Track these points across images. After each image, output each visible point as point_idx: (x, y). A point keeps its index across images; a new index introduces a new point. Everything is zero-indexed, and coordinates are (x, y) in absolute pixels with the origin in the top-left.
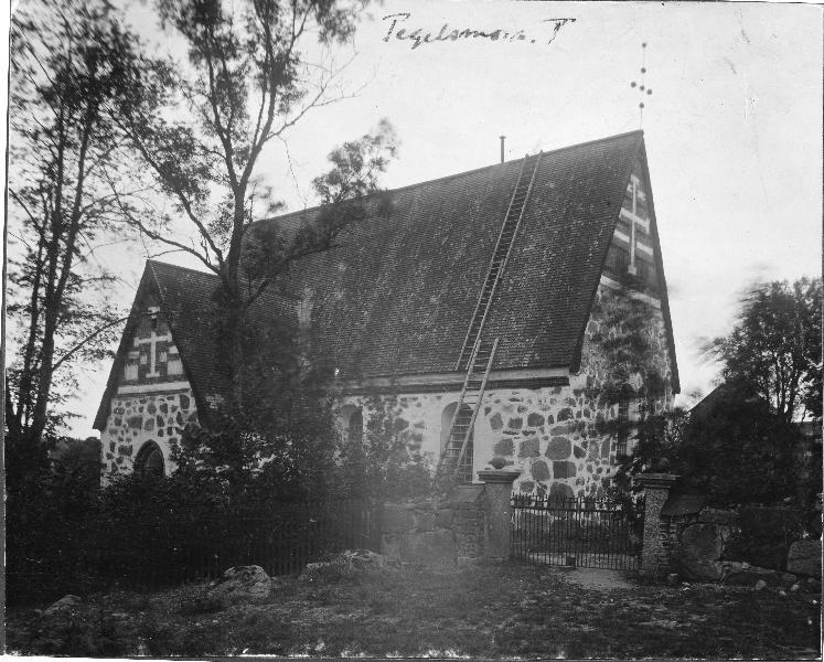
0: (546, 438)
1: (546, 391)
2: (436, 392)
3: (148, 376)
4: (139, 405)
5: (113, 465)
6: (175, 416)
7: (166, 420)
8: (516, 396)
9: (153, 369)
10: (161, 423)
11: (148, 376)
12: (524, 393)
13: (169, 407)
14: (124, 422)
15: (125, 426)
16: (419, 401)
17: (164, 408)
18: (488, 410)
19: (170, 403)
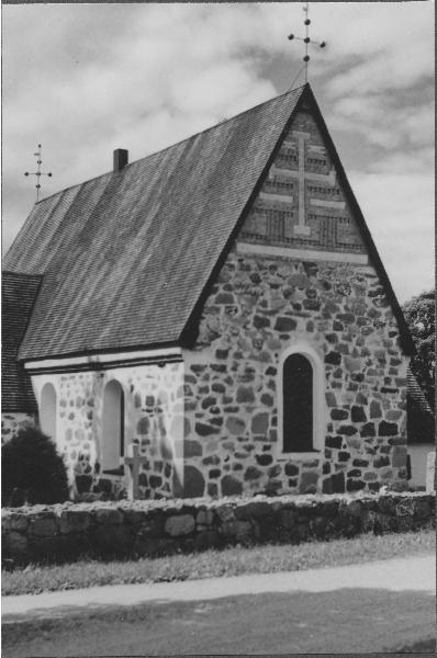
0: (170, 416)
1: (168, 366)
8: (151, 373)
12: (155, 368)
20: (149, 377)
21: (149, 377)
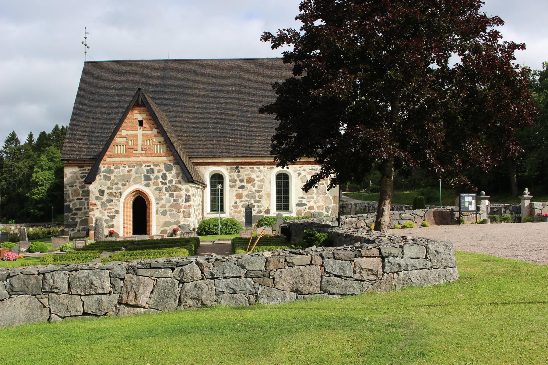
2: (251, 165)
4: (127, 168)
5: (103, 203)
6: (160, 175)
8: (313, 168)
9: (139, 148)
11: (135, 152)
13: (156, 171)
14: (113, 177)
15: (113, 180)
16: (261, 169)
17: (152, 171)
18: (299, 174)
19: (156, 169)
20: (312, 169)
21: (312, 169)
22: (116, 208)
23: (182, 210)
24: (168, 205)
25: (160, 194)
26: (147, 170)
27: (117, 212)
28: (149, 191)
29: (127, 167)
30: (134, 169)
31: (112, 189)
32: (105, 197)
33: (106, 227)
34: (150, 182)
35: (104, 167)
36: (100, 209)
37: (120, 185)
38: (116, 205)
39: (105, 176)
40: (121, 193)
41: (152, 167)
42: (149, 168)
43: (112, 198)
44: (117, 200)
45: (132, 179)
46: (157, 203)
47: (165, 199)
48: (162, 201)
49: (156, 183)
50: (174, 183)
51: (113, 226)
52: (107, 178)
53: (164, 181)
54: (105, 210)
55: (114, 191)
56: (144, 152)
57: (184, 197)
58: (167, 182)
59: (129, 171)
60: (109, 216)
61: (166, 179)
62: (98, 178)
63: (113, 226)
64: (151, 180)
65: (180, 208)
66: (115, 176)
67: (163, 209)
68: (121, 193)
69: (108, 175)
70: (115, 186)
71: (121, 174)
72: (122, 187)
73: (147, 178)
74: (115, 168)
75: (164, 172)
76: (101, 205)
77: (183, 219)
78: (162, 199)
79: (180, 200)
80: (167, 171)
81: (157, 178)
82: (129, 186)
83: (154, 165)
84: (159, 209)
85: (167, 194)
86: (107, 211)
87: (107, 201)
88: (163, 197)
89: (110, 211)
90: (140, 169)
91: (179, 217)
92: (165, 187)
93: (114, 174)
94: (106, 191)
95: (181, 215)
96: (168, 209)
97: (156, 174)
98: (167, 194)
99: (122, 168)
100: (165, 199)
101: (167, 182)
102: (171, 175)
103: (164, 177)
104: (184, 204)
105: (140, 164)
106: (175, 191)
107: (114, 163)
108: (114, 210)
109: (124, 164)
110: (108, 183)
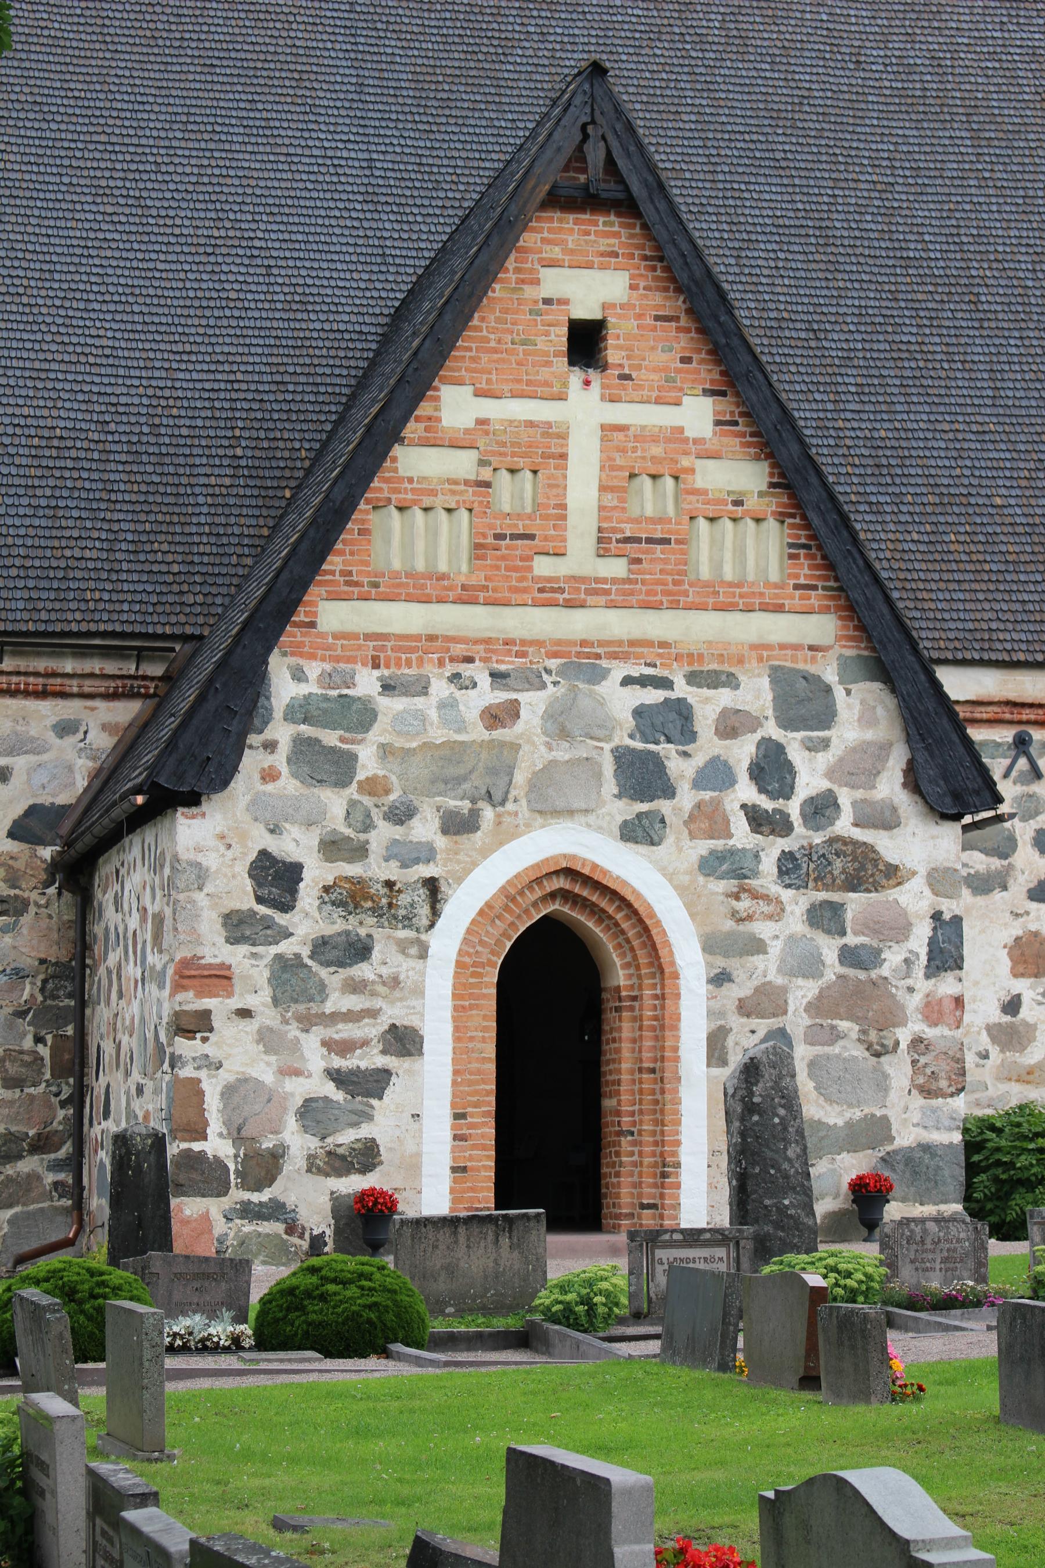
3: (544, 567)
5: (286, 968)
6: (743, 752)
7: (680, 768)
10: (643, 777)
11: (544, 567)
15: (374, 787)
17: (673, 722)
19: (708, 706)
22: (394, 1013)
23: (904, 1036)
24: (803, 992)
25: (745, 904)
26: (639, 712)
27: (404, 1041)
28: (653, 878)
29: (484, 680)
30: (533, 704)
31: (360, 852)
32: (307, 921)
33: (312, 1166)
34: (664, 806)
35: (298, 675)
36: (267, 1016)
37: (425, 828)
38: (395, 982)
39: (303, 748)
40: (432, 886)
41: (682, 689)
42: (653, 696)
43: (363, 926)
44: (403, 947)
45: (520, 778)
46: (720, 979)
47: (775, 948)
48: (758, 960)
49: (708, 820)
50: (844, 825)
51: (366, 1156)
52: (329, 766)
53: (767, 804)
54: (307, 1022)
55: (377, 869)
56: (616, 568)
57: (922, 933)
58: (794, 808)
59: (498, 717)
60: (337, 1077)
61: (786, 792)
62: (251, 762)
63: (366, 1156)
64: (669, 792)
65: (893, 1017)
66: (386, 751)
67: (763, 1026)
68: (432, 886)
69: (331, 738)
70: (383, 833)
71: (438, 735)
72: (441, 842)
73: (643, 777)
74: (388, 688)
75: (772, 730)
76: (275, 981)
77: (918, 1101)
78: (758, 947)
79: (893, 958)
80: (787, 723)
81: (716, 775)
82: (503, 836)
83: (693, 679)
84: (736, 1022)
85: (797, 904)
86: (319, 1033)
87: (321, 946)
88: (763, 929)
89: (344, 1031)
90: (585, 703)
91: (882, 1084)
92: (773, 848)
93: (377, 735)
94: (317, 873)
95: (899, 1070)
96: (797, 1021)
97: (708, 745)
98: (797, 904)
99: (440, 688)
100: (775, 948)
101: (794, 808)
102: (824, 759)
103: (772, 770)
104: (923, 985)
105: (584, 661)
106: (853, 884)
107: (378, 649)
108: (383, 1024)
109: (457, 653)
110: (335, 804)
